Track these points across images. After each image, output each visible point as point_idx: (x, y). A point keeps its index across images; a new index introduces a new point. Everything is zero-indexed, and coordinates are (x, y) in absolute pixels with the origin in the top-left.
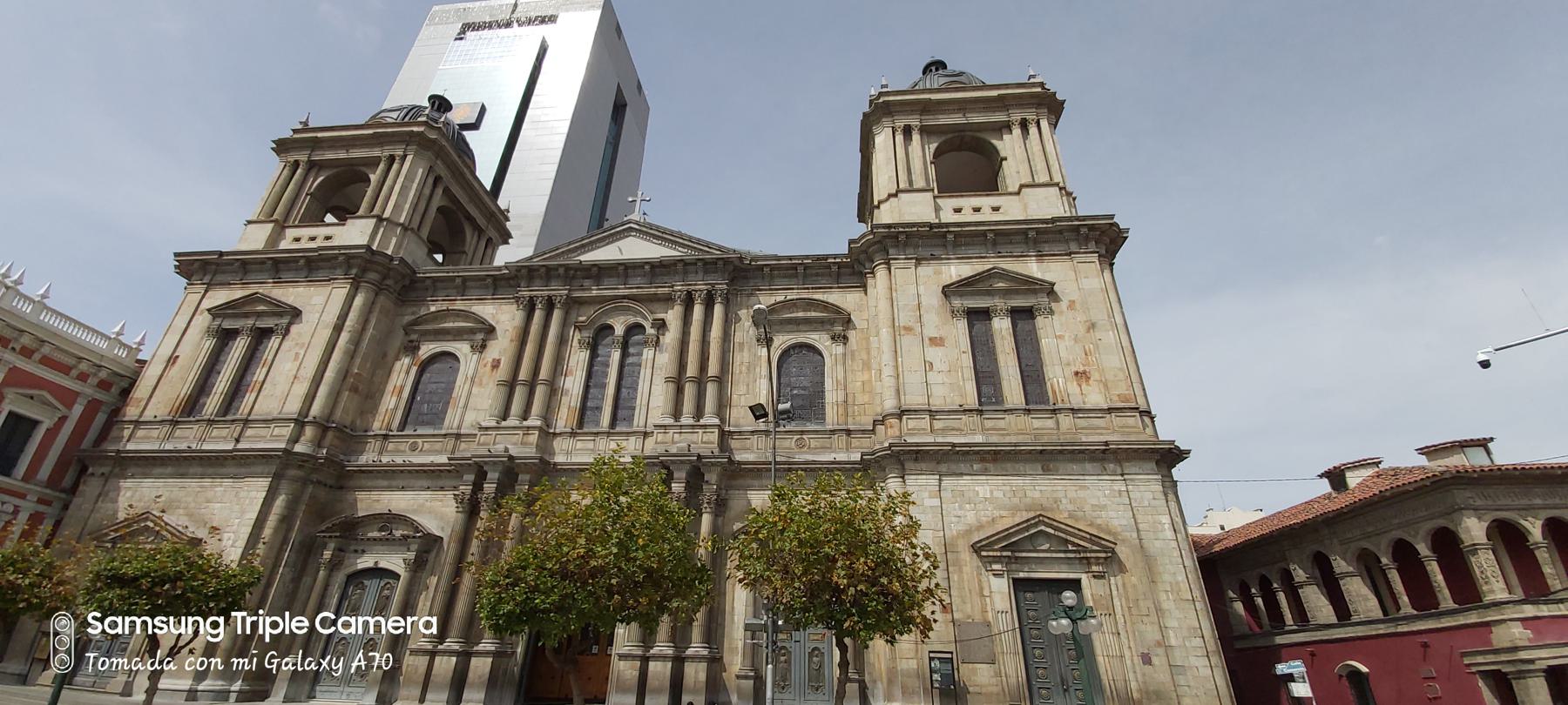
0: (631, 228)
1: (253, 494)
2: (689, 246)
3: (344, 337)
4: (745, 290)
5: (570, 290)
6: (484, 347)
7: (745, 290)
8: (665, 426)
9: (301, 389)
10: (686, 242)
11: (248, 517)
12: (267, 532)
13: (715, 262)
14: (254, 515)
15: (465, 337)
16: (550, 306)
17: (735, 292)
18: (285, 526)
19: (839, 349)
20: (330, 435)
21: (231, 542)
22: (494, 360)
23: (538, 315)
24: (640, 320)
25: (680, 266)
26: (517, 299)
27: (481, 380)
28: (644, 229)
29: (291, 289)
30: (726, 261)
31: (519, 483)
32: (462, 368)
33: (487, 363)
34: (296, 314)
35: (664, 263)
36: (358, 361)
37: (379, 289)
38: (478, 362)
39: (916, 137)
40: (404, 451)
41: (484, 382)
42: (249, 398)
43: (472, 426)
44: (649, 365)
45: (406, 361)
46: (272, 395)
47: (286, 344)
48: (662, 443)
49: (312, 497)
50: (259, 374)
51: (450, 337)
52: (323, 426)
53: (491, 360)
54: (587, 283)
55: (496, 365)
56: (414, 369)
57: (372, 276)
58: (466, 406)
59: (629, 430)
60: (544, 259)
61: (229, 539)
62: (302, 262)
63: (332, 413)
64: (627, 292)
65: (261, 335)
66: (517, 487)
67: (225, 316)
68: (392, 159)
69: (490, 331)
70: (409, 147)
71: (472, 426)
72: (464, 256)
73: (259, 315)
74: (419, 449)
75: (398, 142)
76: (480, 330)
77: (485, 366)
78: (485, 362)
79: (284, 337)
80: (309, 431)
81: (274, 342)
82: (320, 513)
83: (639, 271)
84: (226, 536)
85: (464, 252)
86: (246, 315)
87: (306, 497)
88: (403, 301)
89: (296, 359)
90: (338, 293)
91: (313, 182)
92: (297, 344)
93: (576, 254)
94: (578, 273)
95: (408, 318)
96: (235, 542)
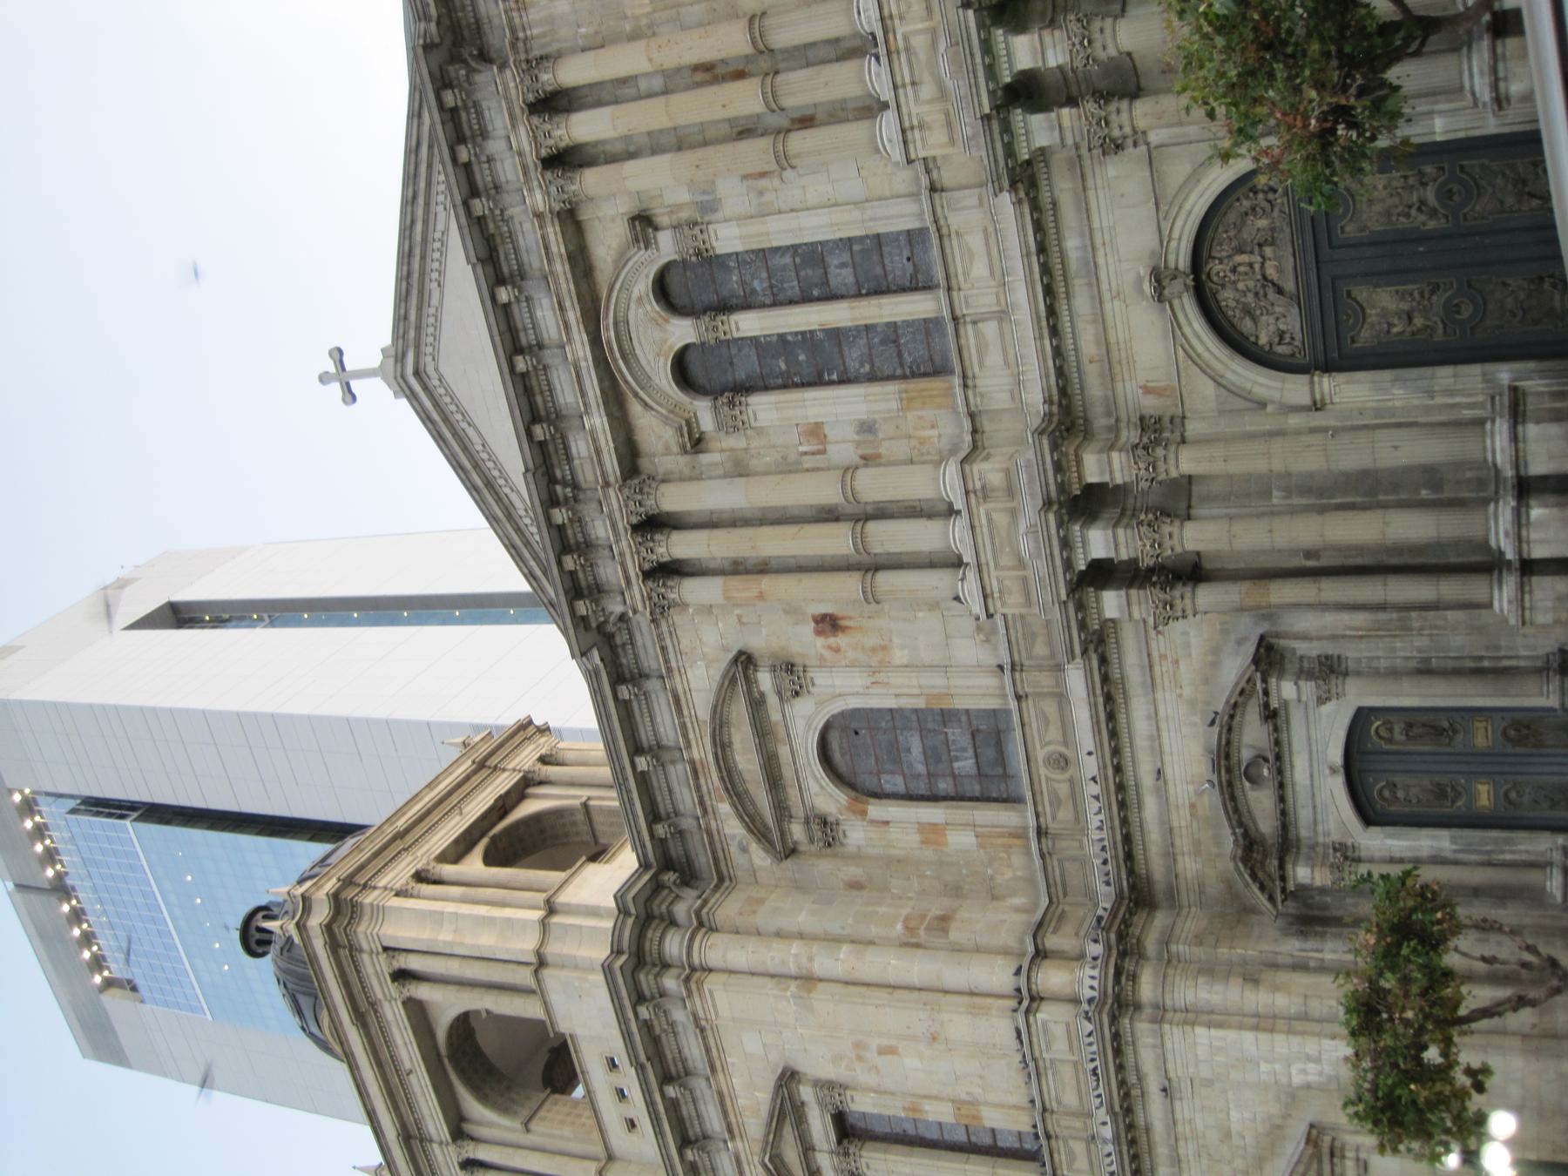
0: (417, 373)
1: (1202, 1052)
2: (427, 204)
3: (824, 962)
4: (510, 20)
5: (607, 484)
6: (790, 667)
7: (510, 20)
8: (903, 131)
9: (959, 1024)
10: (420, 212)
11: (1253, 1048)
12: (1281, 1002)
13: (451, 116)
14: (1249, 1036)
15: (775, 716)
16: (653, 525)
17: (520, 45)
18: (1267, 976)
20: (1052, 942)
21: (1311, 1067)
22: (819, 633)
23: (680, 546)
24: (643, 286)
25: (479, 207)
26: (660, 610)
27: (874, 650)
28: (412, 334)
29: (741, 1102)
30: (442, 83)
31: (1106, 479)
32: (854, 703)
33: (830, 647)
34: (788, 1078)
35: (483, 254)
36: (874, 931)
37: (703, 925)
38: (822, 663)
40: (1071, 781)
41: (872, 641)
42: (993, 1119)
43: (987, 640)
44: (754, 228)
45: (856, 834)
46: (981, 1077)
47: (865, 1078)
48: (949, 124)
49: (1199, 940)
50: (939, 1113)
51: (783, 752)
52: (1041, 954)
53: (820, 641)
54: (580, 447)
55: (829, 624)
56: (876, 810)
57: (673, 945)
58: (945, 668)
59: (932, 229)
60: (545, 573)
61: (1304, 1071)
62: (671, 1091)
63: (1005, 952)
64: (580, 339)
66: (1119, 480)
68: (402, 976)
70: (365, 946)
71: (987, 640)
72: (592, 803)
73: (807, 1149)
74: (1063, 749)
75: (358, 972)
76: (750, 682)
77: (837, 650)
78: (827, 654)
79: (846, 1088)
80: (1052, 978)
81: (862, 1105)
82: (1235, 914)
83: (520, 315)
84: (1297, 1079)
85: (585, 805)
87: (1198, 952)
88: (721, 879)
91: (499, 1126)
92: (859, 1058)
93: (513, 497)
94: (558, 474)
95: (759, 857)
96: (1309, 1058)
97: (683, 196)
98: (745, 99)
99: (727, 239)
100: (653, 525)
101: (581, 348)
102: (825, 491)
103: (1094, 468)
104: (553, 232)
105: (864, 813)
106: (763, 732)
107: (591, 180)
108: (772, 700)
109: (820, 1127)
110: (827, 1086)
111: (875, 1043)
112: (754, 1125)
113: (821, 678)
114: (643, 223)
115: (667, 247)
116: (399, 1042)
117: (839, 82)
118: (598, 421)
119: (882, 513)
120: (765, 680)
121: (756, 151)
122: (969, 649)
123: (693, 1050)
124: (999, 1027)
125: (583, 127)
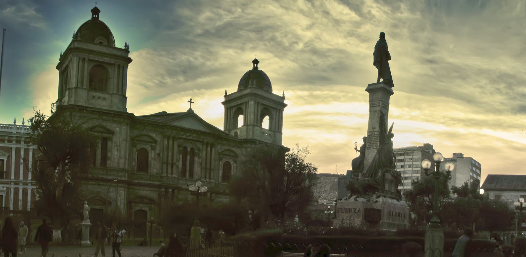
0: (192, 115)
6: (155, 148)
15: (149, 144)
16: (174, 139)
19: (235, 165)
23: (171, 142)
29: (108, 124)
32: (150, 156)
33: (156, 154)
34: (113, 133)
38: (155, 152)
39: (259, 105)
45: (134, 149)
47: (113, 145)
50: (109, 154)
54: (182, 133)
55: (159, 155)
56: (137, 153)
65: (105, 140)
67: (91, 131)
69: (156, 142)
73: (102, 132)
76: (154, 143)
81: (109, 144)
86: (98, 132)
89: (117, 150)
90: (124, 128)
97: (201, 155)
98: (208, 166)
99: (196, 158)
100: (174, 139)
101: (191, 138)
102: (175, 161)
103: (176, 191)
104: (201, 140)
105: (136, 151)
106: (147, 142)
107: (205, 147)
108: (151, 144)
109: (105, 135)
110: (111, 139)
111: (119, 148)
112: (104, 124)
113: (153, 152)
114: (199, 150)
115: (197, 151)
116: (108, 59)
117: (208, 176)
118: (184, 137)
119: (172, 166)
120: (154, 144)
121: (204, 166)
122: (155, 171)
123: (116, 119)
124: (122, 166)
125: (209, 148)
